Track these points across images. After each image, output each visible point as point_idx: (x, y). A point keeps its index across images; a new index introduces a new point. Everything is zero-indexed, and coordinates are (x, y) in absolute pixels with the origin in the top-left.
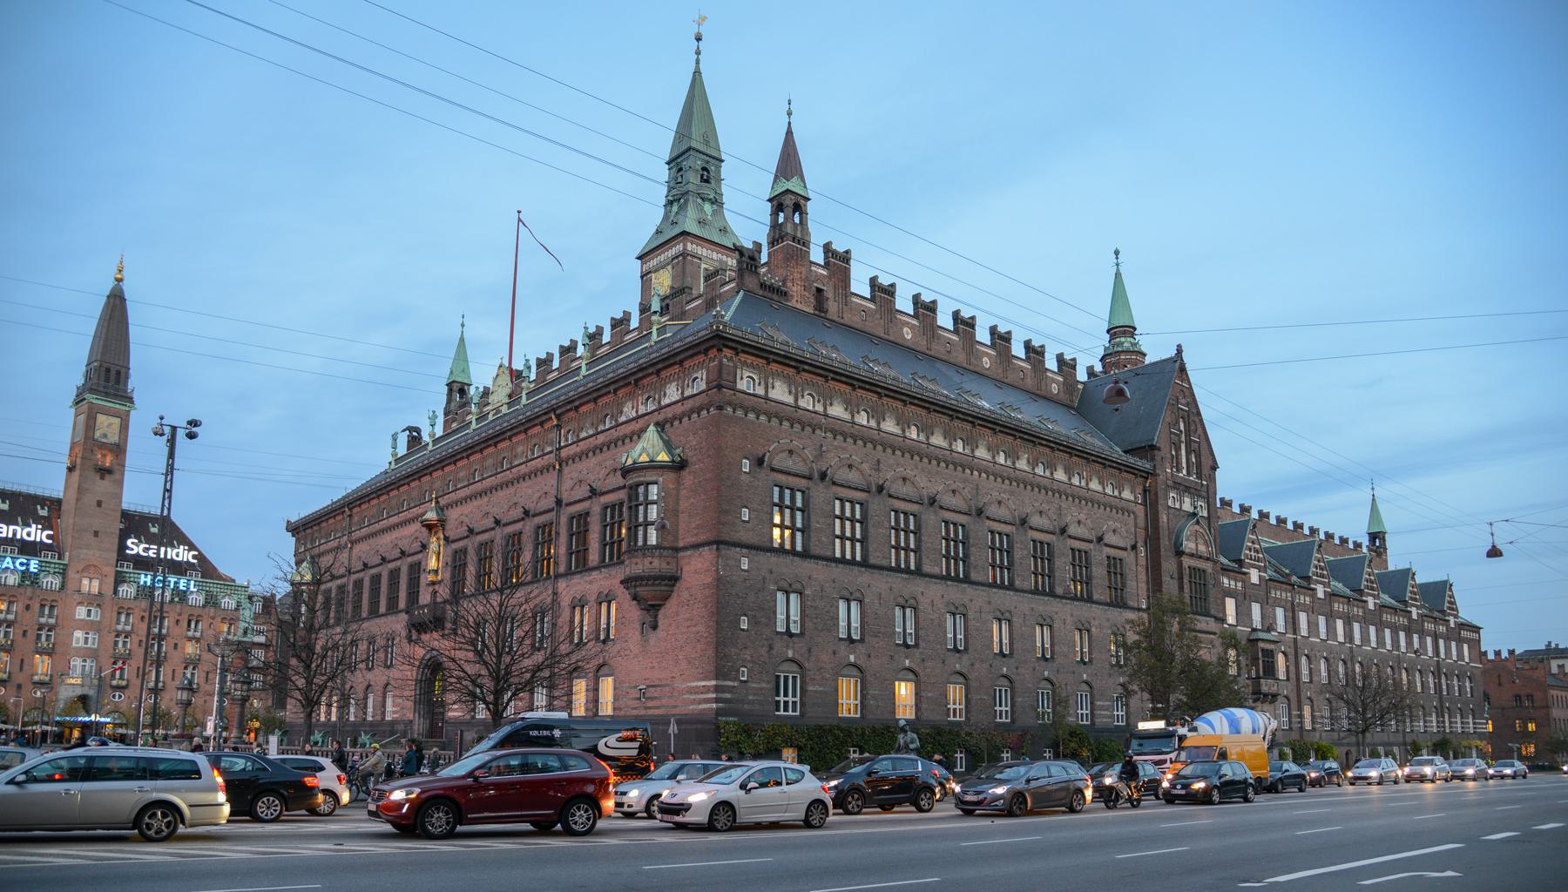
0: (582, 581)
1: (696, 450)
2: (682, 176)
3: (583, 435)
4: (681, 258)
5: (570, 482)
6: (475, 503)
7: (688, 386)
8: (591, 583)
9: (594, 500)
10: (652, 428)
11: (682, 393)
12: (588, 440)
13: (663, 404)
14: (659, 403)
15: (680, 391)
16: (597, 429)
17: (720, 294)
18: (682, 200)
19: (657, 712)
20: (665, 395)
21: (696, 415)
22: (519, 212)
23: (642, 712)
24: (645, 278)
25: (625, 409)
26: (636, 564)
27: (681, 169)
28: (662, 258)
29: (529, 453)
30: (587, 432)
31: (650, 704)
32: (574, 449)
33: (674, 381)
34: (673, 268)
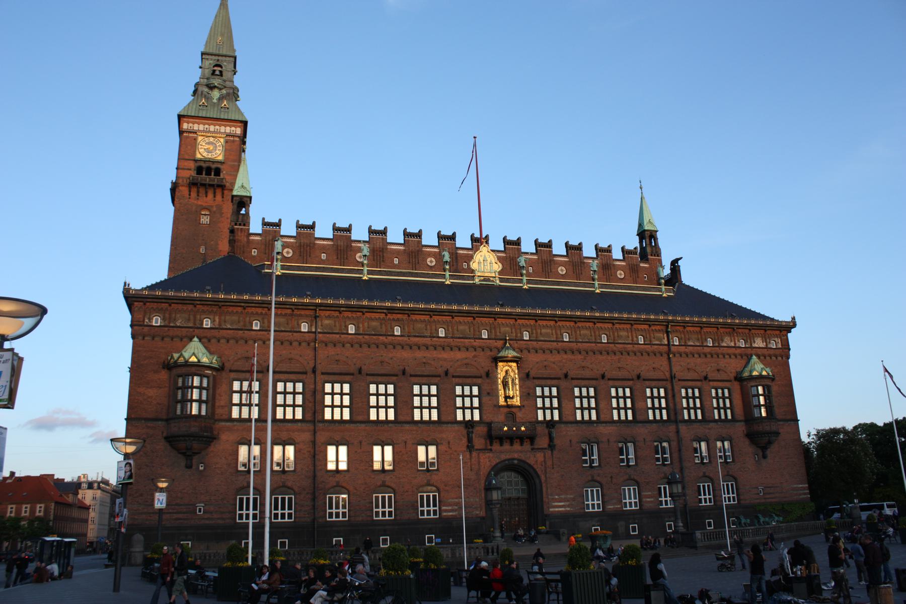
2: (221, 72)
3: (692, 343)
6: (570, 356)
7: (770, 342)
8: (709, 429)
9: (704, 382)
10: (754, 357)
11: (767, 345)
12: (695, 348)
14: (751, 345)
15: (765, 344)
16: (702, 343)
17: (614, 265)
18: (224, 91)
20: (754, 342)
21: (780, 358)
22: (475, 137)
23: (763, 501)
25: (725, 340)
27: (221, 67)
28: (212, 128)
29: (635, 339)
31: (768, 496)
32: (682, 349)
33: (759, 337)
34: (226, 142)
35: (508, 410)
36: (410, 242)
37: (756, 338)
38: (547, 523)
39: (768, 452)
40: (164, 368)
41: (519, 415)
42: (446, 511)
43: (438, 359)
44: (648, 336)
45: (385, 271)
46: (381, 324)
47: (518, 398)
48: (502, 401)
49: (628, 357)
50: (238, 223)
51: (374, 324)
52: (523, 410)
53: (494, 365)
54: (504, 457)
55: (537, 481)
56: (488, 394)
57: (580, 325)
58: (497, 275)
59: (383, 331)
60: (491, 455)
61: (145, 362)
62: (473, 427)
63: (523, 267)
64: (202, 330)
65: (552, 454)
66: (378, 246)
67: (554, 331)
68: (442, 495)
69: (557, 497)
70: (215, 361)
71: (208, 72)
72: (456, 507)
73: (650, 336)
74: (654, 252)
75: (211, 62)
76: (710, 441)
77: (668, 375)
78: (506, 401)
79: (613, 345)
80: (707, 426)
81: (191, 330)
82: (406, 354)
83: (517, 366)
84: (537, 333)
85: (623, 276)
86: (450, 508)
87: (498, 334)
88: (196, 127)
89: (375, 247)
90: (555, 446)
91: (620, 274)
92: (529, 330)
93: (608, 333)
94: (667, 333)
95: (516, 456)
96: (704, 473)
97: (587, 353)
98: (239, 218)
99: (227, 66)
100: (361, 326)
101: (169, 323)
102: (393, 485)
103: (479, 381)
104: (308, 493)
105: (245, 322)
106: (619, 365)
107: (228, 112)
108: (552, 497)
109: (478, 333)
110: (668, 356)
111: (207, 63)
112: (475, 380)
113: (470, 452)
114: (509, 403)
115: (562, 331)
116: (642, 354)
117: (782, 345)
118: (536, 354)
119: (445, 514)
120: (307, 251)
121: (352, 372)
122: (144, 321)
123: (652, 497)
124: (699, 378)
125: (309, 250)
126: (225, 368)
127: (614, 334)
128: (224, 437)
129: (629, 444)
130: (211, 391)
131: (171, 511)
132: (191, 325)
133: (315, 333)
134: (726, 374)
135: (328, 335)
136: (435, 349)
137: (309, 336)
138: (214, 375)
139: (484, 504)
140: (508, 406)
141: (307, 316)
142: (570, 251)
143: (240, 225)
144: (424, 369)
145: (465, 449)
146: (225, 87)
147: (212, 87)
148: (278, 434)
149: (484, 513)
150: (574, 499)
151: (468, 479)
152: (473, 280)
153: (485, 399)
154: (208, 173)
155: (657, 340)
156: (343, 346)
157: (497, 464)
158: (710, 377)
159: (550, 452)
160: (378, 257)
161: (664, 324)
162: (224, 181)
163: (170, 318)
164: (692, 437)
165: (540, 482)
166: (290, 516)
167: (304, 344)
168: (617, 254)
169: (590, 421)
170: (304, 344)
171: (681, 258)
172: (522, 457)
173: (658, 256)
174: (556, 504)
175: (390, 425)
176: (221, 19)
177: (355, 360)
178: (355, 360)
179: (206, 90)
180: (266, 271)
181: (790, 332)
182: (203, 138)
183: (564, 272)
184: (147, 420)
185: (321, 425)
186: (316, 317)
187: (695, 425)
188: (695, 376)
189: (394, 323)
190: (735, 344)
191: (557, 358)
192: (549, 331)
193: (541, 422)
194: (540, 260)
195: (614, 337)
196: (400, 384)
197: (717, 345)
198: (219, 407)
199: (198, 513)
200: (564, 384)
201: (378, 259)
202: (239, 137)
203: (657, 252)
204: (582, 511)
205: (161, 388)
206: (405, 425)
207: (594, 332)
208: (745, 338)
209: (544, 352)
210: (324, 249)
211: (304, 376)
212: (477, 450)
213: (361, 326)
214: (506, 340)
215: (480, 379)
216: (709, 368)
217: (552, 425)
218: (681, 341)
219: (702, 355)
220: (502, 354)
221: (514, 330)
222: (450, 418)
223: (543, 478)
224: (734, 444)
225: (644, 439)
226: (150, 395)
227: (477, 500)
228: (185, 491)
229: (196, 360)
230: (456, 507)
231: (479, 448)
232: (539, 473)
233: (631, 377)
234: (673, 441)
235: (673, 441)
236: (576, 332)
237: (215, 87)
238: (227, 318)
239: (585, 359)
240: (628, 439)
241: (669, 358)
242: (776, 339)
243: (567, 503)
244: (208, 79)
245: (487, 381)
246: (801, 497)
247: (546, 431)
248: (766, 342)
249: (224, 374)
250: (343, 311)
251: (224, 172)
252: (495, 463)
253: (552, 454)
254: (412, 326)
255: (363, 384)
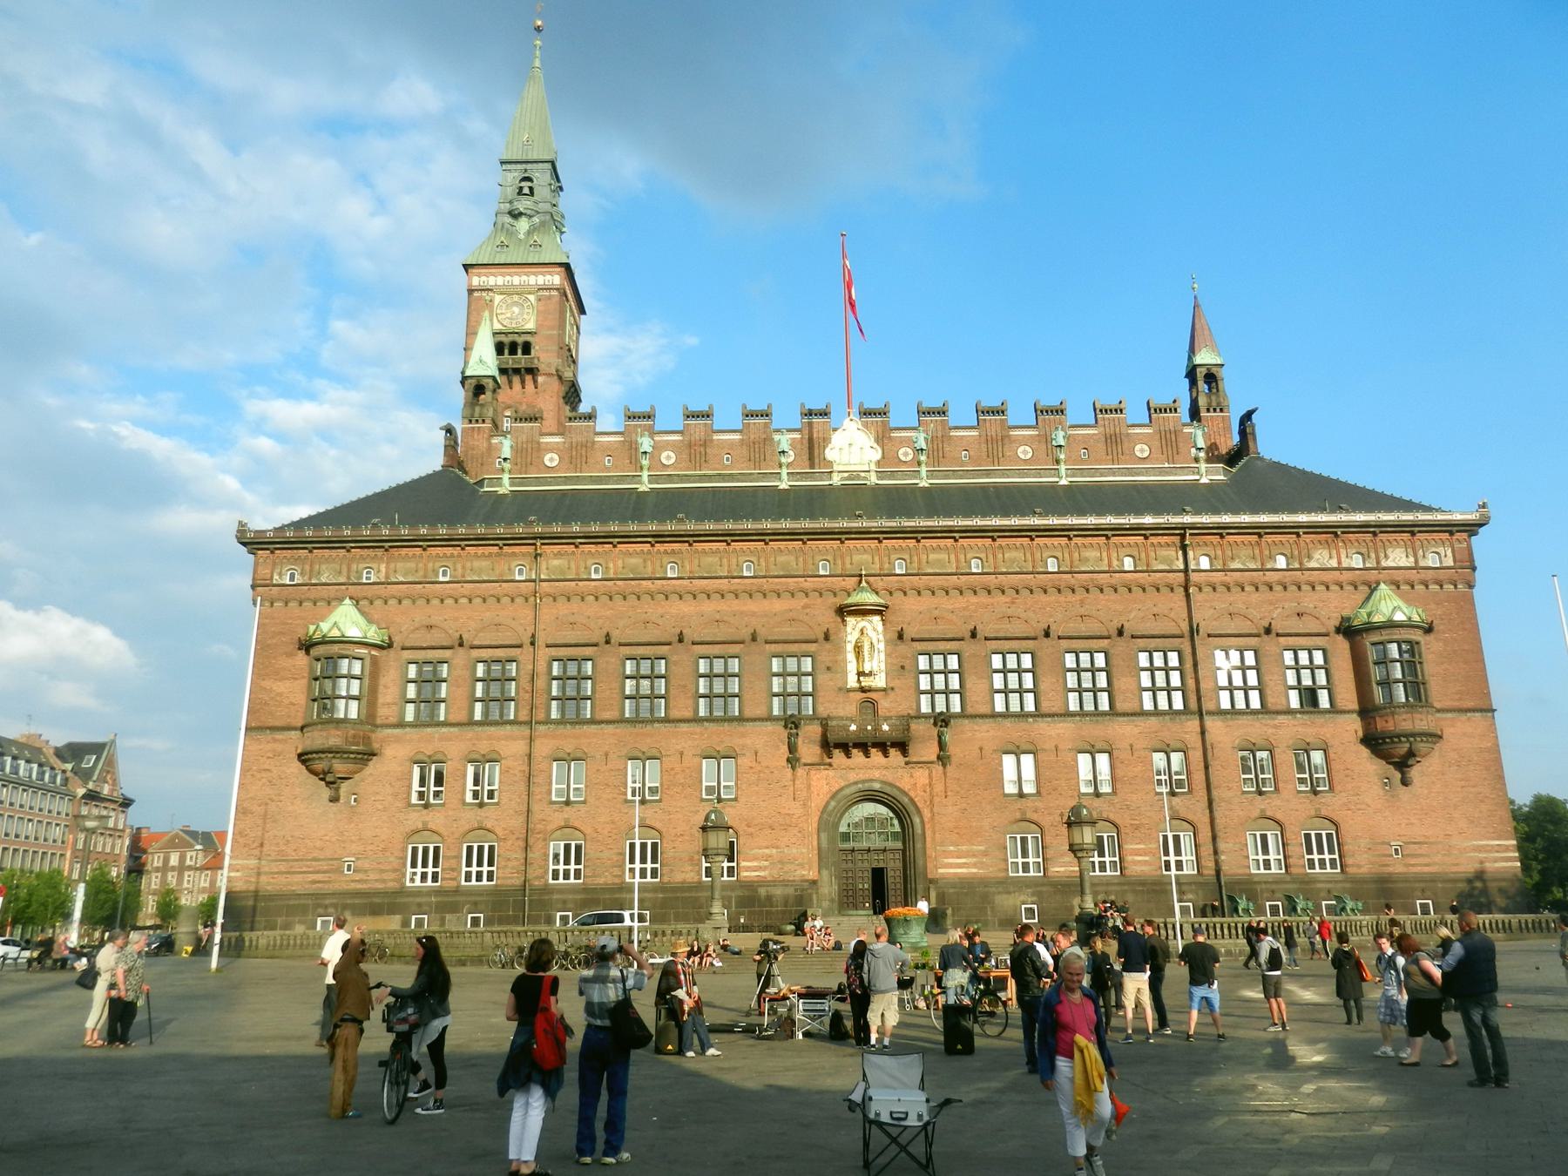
0: (1257, 724)
1: (1442, 619)
2: (531, 189)
4: (555, 293)
5: (1212, 611)
6: (983, 598)
7: (1424, 556)
8: (1275, 727)
9: (1265, 637)
11: (1416, 561)
13: (1384, 564)
15: (1412, 559)
17: (1128, 434)
18: (536, 220)
19: (1426, 869)
20: (1386, 557)
24: (476, 294)
25: (1316, 556)
26: (1421, 720)
28: (516, 280)
29: (1115, 562)
30: (1244, 564)
32: (1218, 577)
33: (1398, 546)
35: (864, 695)
36: (752, 426)
37: (1389, 551)
38: (933, 895)
39: (1415, 772)
40: (299, 649)
41: (885, 705)
42: (748, 869)
43: (742, 613)
44: (1143, 555)
45: (678, 475)
46: (645, 561)
47: (883, 675)
48: (852, 681)
49: (1101, 596)
50: (474, 419)
51: (634, 561)
52: (892, 694)
53: (839, 620)
54: (853, 777)
55: (917, 820)
56: (828, 668)
57: (1003, 544)
58: (873, 467)
59: (648, 572)
60: (831, 773)
61: (274, 641)
62: (796, 727)
63: (922, 450)
64: (360, 587)
65: (945, 774)
66: (698, 438)
67: (952, 557)
68: (741, 842)
69: (952, 848)
70: (373, 634)
71: (511, 192)
72: (766, 863)
73: (1147, 556)
74: (1214, 404)
75: (516, 174)
76: (1277, 751)
77: (1185, 627)
78: (859, 681)
79: (1070, 576)
80: (1271, 722)
81: (344, 587)
82: (687, 607)
83: (883, 620)
84: (919, 561)
85: (1146, 454)
86: (755, 864)
87: (848, 566)
88: (492, 281)
89: (693, 439)
90: (949, 757)
91: (1141, 450)
92: (906, 557)
93: (1059, 555)
94: (1184, 548)
95: (876, 774)
96: (1263, 811)
97: (1017, 592)
98: (474, 411)
99: (541, 177)
100: (611, 565)
101: (310, 579)
102: (658, 825)
103: (812, 647)
104: (518, 839)
105: (426, 570)
106: (1082, 611)
107: (540, 252)
108: (943, 848)
109: (811, 567)
110: (1186, 589)
111: (510, 176)
112: (805, 647)
113: (793, 768)
114: (863, 684)
115: (969, 556)
116: (1130, 590)
117: (1455, 561)
118: (919, 598)
119: (746, 874)
120: (581, 455)
121: (594, 640)
122: (272, 578)
123: (1145, 854)
124: (1255, 631)
125: (584, 453)
126: (395, 645)
127: (1071, 556)
128: (389, 752)
129: (1259, 754)
130: (366, 681)
131: (305, 869)
132: (342, 580)
133: (534, 581)
134: (1318, 622)
135: (557, 584)
136: (737, 596)
137: (526, 587)
138: (373, 657)
139: (816, 858)
140: (863, 690)
141: (524, 555)
142: (1040, 418)
143: (477, 421)
144: (717, 630)
145: (784, 763)
146: (538, 213)
147: (515, 215)
148: (474, 744)
149: (816, 873)
150: (985, 853)
151: (789, 815)
152: (831, 479)
153: (823, 677)
154: (513, 351)
155: (1161, 563)
156: (583, 599)
157: (842, 789)
158: (1277, 627)
159: (941, 768)
160: (698, 456)
161: (1178, 532)
162: (536, 361)
163: (311, 571)
164: (1237, 742)
165: (923, 822)
166: (435, 877)
167: (519, 600)
168: (1136, 413)
169: (1022, 715)
170: (519, 600)
171: (1256, 409)
172: (889, 776)
173: (1221, 410)
174: (951, 861)
175: (656, 725)
176: (529, 102)
177: (600, 621)
178: (600, 621)
179: (508, 219)
180: (486, 489)
181: (1475, 533)
182: (502, 297)
183: (1030, 455)
184: (273, 729)
185: (542, 728)
186: (536, 557)
187: (1244, 720)
188: (1247, 627)
189: (666, 559)
190: (1339, 563)
191: (957, 602)
192: (944, 556)
193: (926, 716)
194: (983, 439)
195: (1072, 562)
196: (675, 658)
197: (1297, 566)
198: (384, 704)
199: (346, 872)
200: (968, 647)
201: (698, 458)
202: (557, 289)
203: (1218, 404)
204: (1002, 875)
205: (296, 679)
206: (682, 725)
207: (1032, 555)
208: (1364, 550)
209: (933, 593)
210: (609, 450)
211: (518, 651)
212: (805, 765)
213: (611, 565)
214: (861, 575)
215: (815, 645)
216: (1280, 610)
217: (943, 721)
218: (1215, 563)
219: (1262, 588)
220: (850, 601)
221: (876, 559)
222: (760, 711)
223: (926, 813)
224: (1332, 756)
225: (1131, 746)
226: (279, 691)
227: (804, 851)
228: (327, 838)
229: (338, 634)
230: (766, 863)
231: (809, 762)
232: (920, 805)
233: (1106, 634)
234: (1194, 749)
235: (1194, 749)
236: (995, 556)
237: (521, 214)
238: (400, 565)
239: (1013, 603)
240: (1099, 746)
241: (1188, 595)
242: (1441, 550)
243: (973, 860)
244: (511, 202)
245: (828, 646)
246: (1497, 865)
247: (935, 731)
248: (1415, 556)
249: (392, 651)
250: (581, 543)
251: (537, 348)
252: (837, 787)
253: (945, 774)
254: (696, 562)
255: (613, 660)
